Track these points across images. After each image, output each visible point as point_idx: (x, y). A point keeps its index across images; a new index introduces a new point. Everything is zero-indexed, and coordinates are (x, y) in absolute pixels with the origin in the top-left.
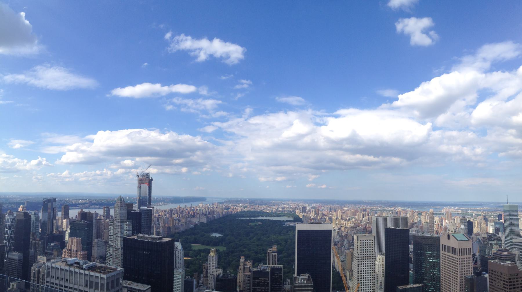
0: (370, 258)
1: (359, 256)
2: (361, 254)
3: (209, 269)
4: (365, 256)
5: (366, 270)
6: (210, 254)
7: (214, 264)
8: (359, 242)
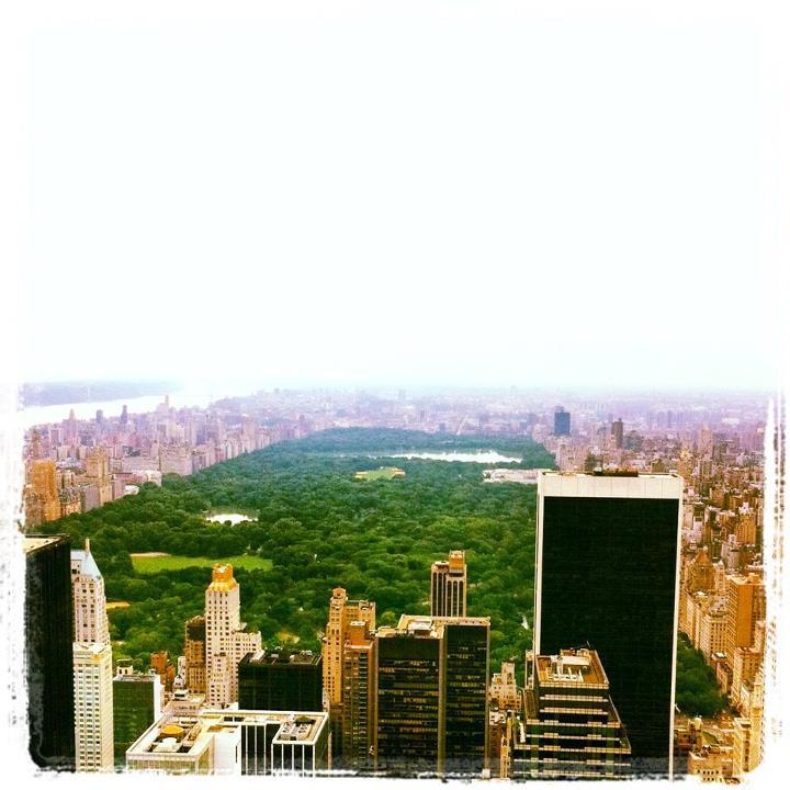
3: (208, 636)
6: (212, 585)
7: (227, 618)
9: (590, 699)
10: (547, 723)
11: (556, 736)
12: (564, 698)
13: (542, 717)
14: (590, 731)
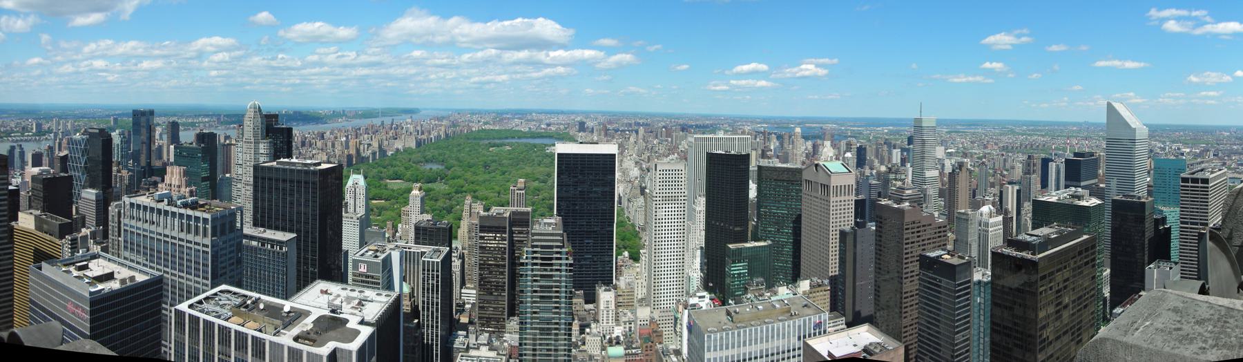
0: (676, 198)
1: (658, 195)
2: (661, 191)
4: (667, 195)
8: (658, 172)
9: (554, 238)
10: (535, 249)
12: (542, 238)
13: (533, 247)
14: (553, 253)
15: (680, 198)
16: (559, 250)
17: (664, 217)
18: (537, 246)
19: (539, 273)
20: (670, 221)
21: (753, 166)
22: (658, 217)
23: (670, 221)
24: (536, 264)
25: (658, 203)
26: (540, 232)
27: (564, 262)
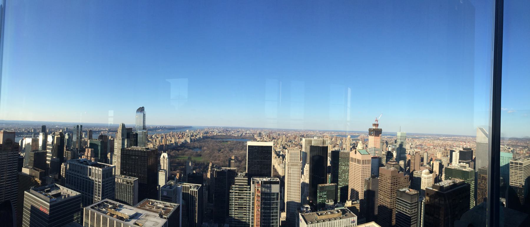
0: (297, 165)
1: (289, 163)
2: (290, 162)
4: (293, 163)
5: (294, 173)
8: (289, 154)
9: (244, 181)
10: (236, 186)
11: (238, 189)
15: (298, 165)
16: (246, 186)
17: (292, 173)
18: (237, 185)
19: (238, 196)
20: (294, 174)
21: (329, 151)
22: (289, 173)
23: (294, 174)
24: (237, 193)
25: (289, 167)
26: (238, 178)
27: (248, 192)
